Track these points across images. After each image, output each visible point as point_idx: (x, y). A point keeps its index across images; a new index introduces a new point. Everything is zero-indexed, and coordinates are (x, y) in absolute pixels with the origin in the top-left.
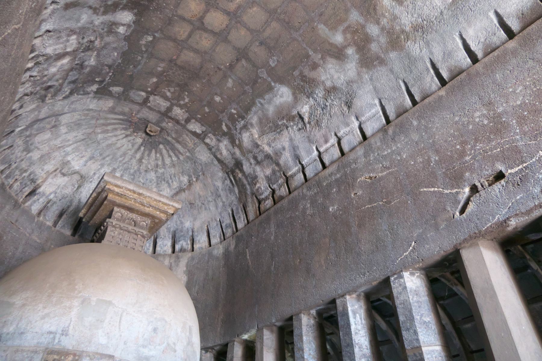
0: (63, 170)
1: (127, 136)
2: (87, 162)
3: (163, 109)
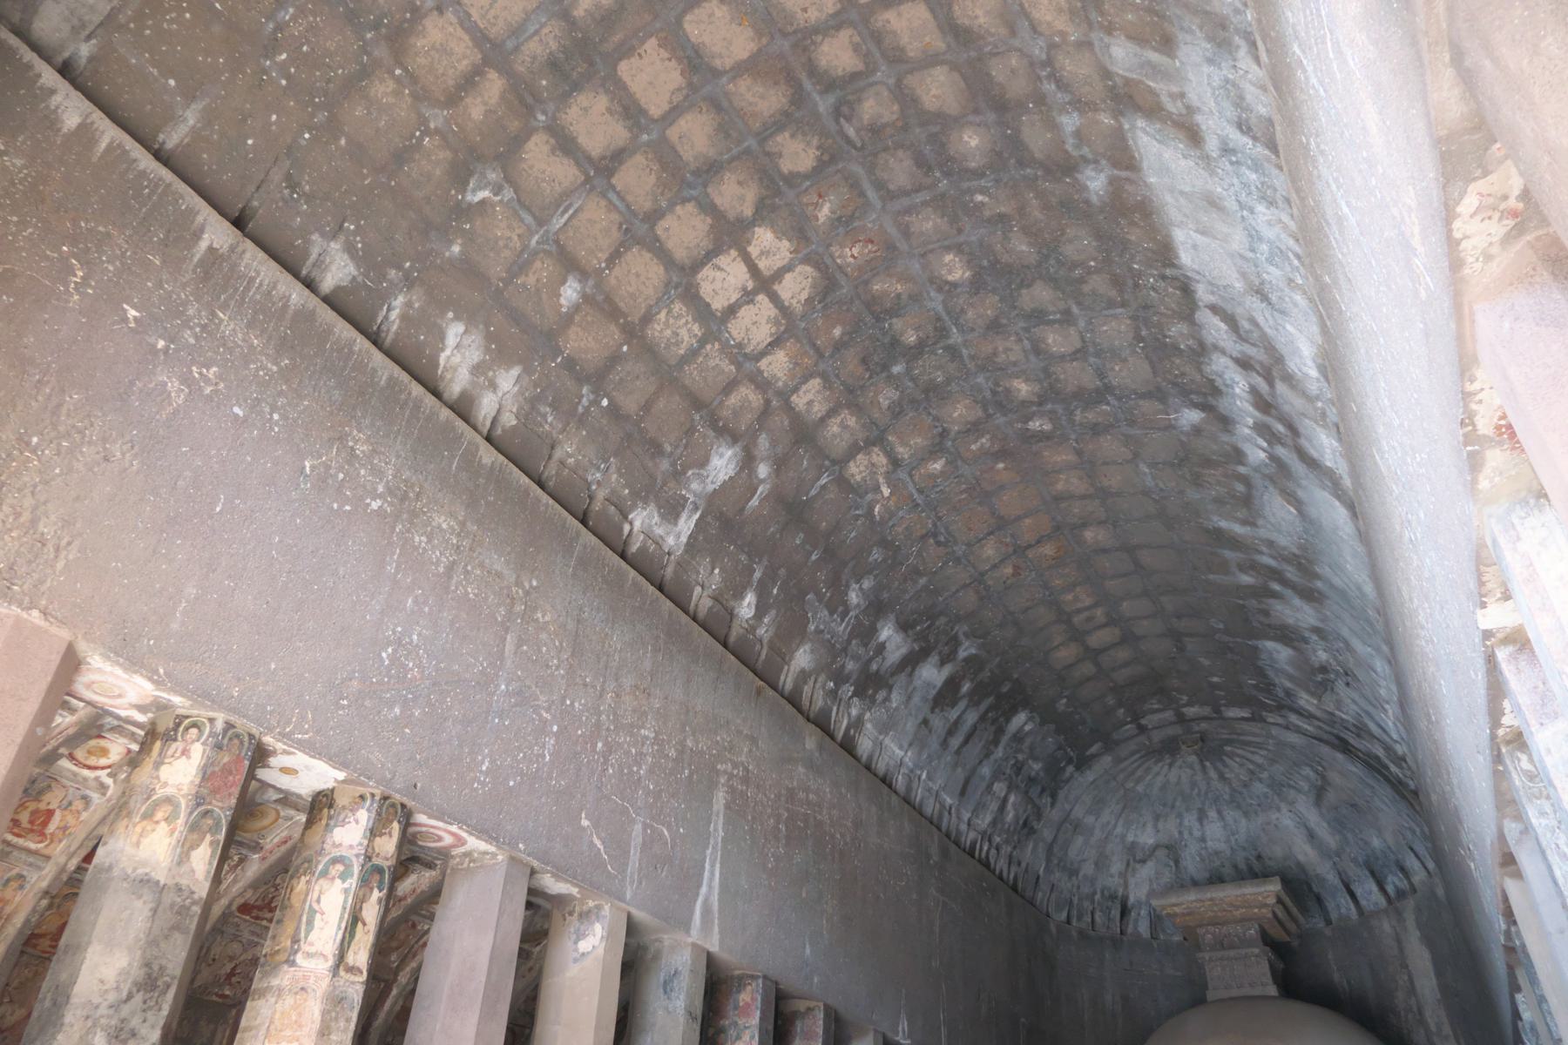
0: (1135, 856)
1: (1171, 765)
2: (1155, 826)
3: (1174, 719)
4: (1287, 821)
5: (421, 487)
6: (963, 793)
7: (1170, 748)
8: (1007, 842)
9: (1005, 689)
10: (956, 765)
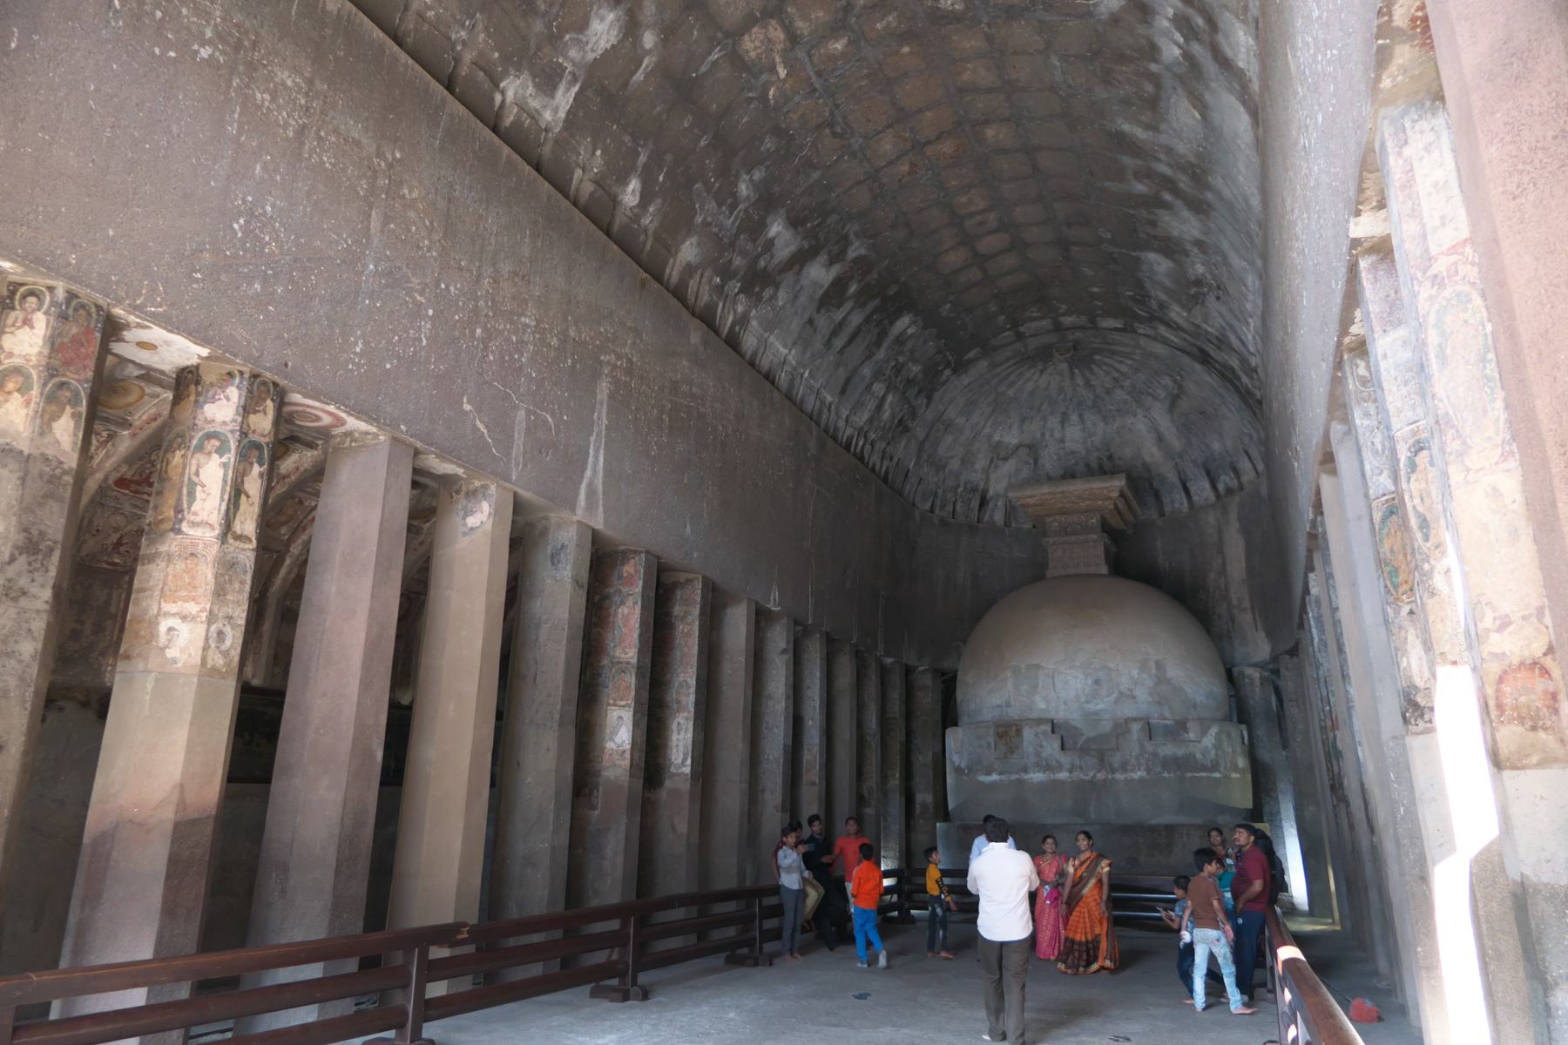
0: (999, 454)
1: (1042, 372)
2: (1021, 427)
4: (1140, 425)
5: (257, 34)
6: (843, 392)
7: (1044, 356)
8: (881, 438)
9: (891, 292)
10: (838, 365)
